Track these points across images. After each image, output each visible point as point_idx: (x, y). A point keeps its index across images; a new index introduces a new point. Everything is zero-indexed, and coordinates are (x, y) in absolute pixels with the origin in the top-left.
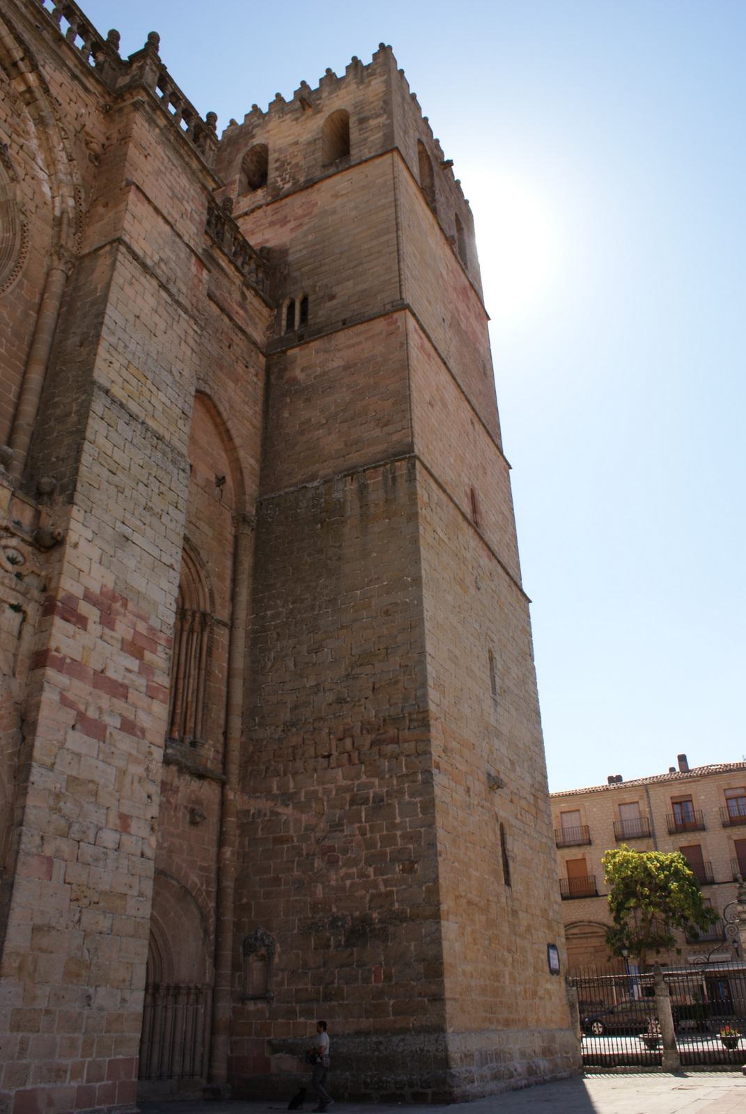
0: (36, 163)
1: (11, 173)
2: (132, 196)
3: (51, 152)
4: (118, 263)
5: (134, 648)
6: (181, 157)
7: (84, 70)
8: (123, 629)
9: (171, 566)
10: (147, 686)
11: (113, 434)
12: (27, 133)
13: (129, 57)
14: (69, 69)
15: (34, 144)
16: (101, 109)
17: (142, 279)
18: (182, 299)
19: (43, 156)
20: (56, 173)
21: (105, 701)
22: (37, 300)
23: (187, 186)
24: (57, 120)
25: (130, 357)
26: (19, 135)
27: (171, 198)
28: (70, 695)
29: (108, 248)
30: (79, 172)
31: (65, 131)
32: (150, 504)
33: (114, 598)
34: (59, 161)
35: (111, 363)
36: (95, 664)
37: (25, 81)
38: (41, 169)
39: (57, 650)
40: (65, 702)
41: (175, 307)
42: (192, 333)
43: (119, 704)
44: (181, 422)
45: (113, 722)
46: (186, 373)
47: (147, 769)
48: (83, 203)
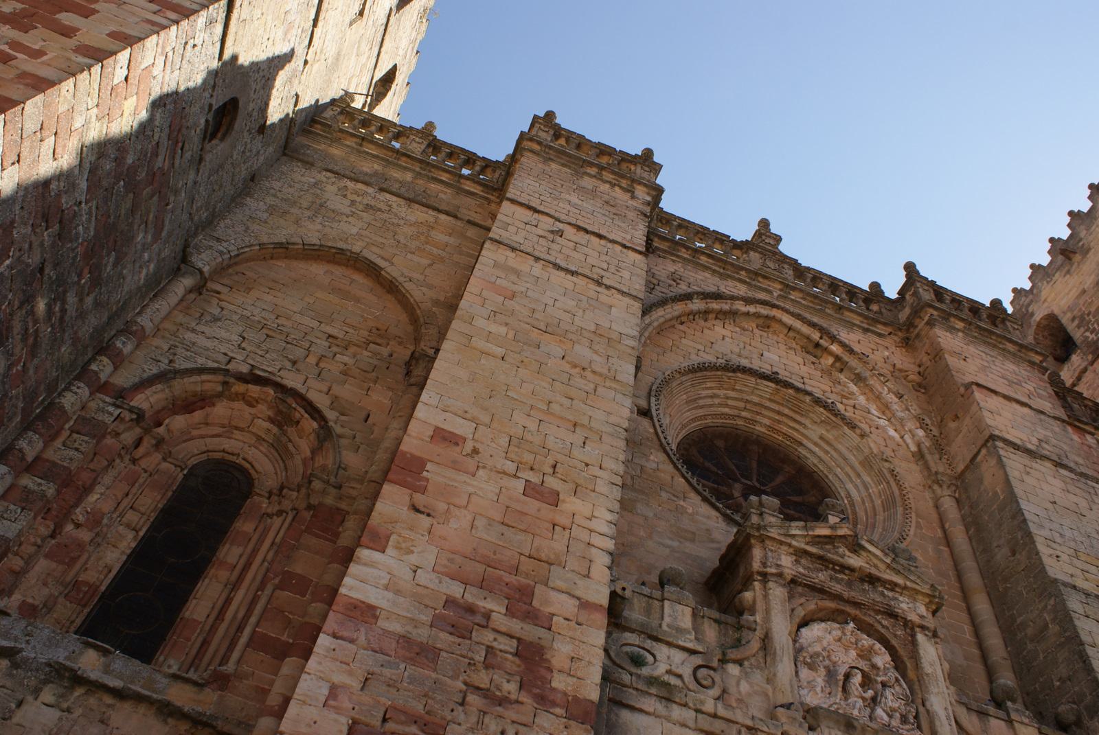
0: (873, 415)
1: (858, 431)
2: (978, 395)
3: (880, 399)
4: (1004, 459)
6: (994, 346)
7: (870, 321)
12: (853, 393)
13: (898, 293)
14: (859, 327)
15: (862, 400)
16: (901, 345)
17: (1034, 465)
18: (1083, 470)
19: (875, 407)
20: (894, 414)
22: (939, 533)
24: (871, 370)
26: (847, 398)
29: (984, 451)
30: (913, 403)
31: (882, 375)
34: (891, 403)
35: (1057, 557)
37: (831, 353)
38: (879, 418)
48: (932, 428)
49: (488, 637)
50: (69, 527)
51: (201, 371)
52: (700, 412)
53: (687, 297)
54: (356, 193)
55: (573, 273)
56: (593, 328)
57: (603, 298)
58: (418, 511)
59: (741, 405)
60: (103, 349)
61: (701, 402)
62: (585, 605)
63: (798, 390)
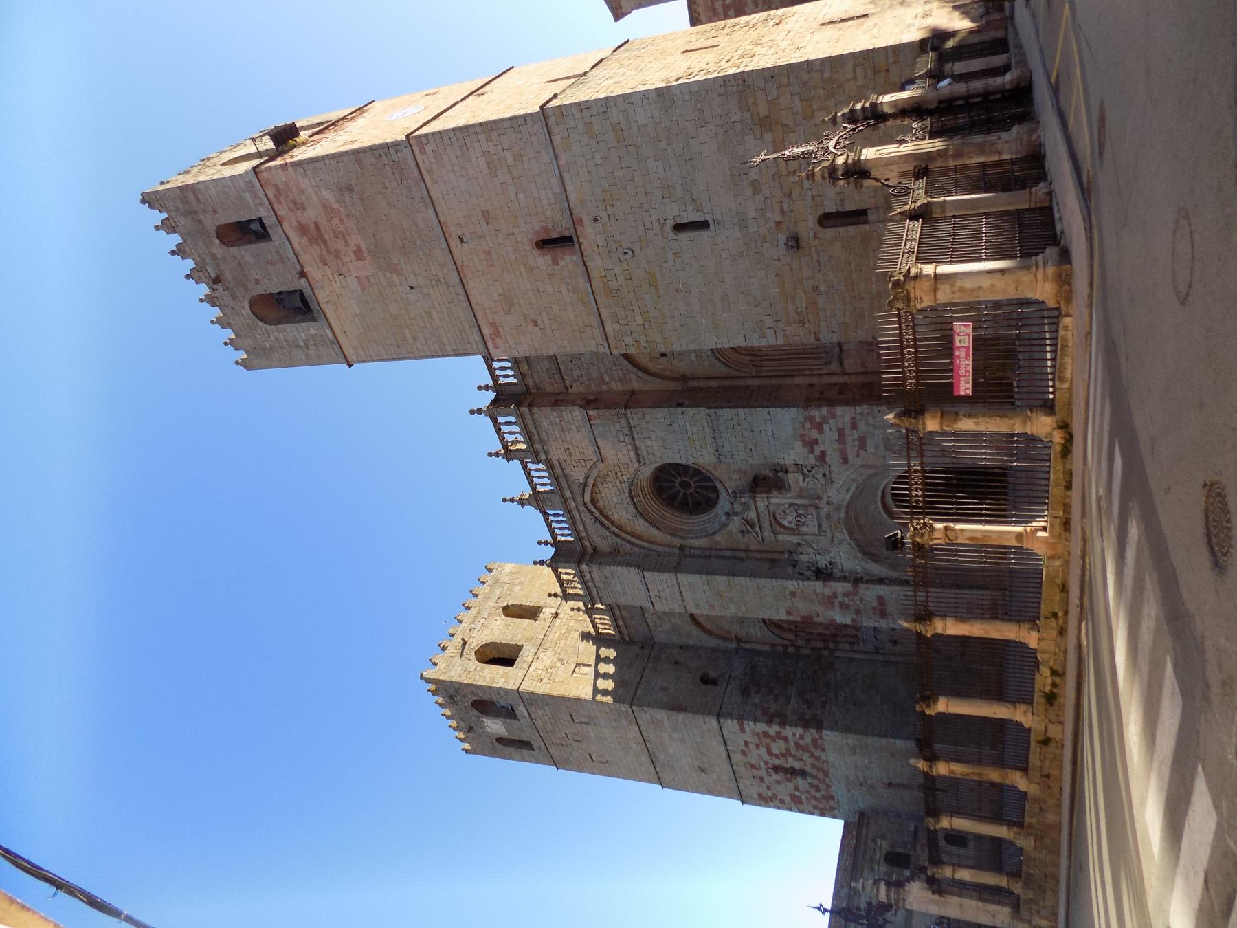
5: (819, 427)
8: (814, 434)
10: (832, 418)
17: (643, 448)
18: (624, 424)
21: (849, 439)
25: (689, 448)
33: (804, 441)
36: (836, 445)
40: (858, 456)
41: (633, 429)
43: (847, 432)
44: (691, 414)
45: (856, 434)
46: (660, 416)
47: (868, 414)
50: (833, 632)
51: (771, 631)
53: (614, 533)
54: (655, 623)
55: (681, 592)
60: (786, 653)
62: (824, 585)
63: (630, 490)
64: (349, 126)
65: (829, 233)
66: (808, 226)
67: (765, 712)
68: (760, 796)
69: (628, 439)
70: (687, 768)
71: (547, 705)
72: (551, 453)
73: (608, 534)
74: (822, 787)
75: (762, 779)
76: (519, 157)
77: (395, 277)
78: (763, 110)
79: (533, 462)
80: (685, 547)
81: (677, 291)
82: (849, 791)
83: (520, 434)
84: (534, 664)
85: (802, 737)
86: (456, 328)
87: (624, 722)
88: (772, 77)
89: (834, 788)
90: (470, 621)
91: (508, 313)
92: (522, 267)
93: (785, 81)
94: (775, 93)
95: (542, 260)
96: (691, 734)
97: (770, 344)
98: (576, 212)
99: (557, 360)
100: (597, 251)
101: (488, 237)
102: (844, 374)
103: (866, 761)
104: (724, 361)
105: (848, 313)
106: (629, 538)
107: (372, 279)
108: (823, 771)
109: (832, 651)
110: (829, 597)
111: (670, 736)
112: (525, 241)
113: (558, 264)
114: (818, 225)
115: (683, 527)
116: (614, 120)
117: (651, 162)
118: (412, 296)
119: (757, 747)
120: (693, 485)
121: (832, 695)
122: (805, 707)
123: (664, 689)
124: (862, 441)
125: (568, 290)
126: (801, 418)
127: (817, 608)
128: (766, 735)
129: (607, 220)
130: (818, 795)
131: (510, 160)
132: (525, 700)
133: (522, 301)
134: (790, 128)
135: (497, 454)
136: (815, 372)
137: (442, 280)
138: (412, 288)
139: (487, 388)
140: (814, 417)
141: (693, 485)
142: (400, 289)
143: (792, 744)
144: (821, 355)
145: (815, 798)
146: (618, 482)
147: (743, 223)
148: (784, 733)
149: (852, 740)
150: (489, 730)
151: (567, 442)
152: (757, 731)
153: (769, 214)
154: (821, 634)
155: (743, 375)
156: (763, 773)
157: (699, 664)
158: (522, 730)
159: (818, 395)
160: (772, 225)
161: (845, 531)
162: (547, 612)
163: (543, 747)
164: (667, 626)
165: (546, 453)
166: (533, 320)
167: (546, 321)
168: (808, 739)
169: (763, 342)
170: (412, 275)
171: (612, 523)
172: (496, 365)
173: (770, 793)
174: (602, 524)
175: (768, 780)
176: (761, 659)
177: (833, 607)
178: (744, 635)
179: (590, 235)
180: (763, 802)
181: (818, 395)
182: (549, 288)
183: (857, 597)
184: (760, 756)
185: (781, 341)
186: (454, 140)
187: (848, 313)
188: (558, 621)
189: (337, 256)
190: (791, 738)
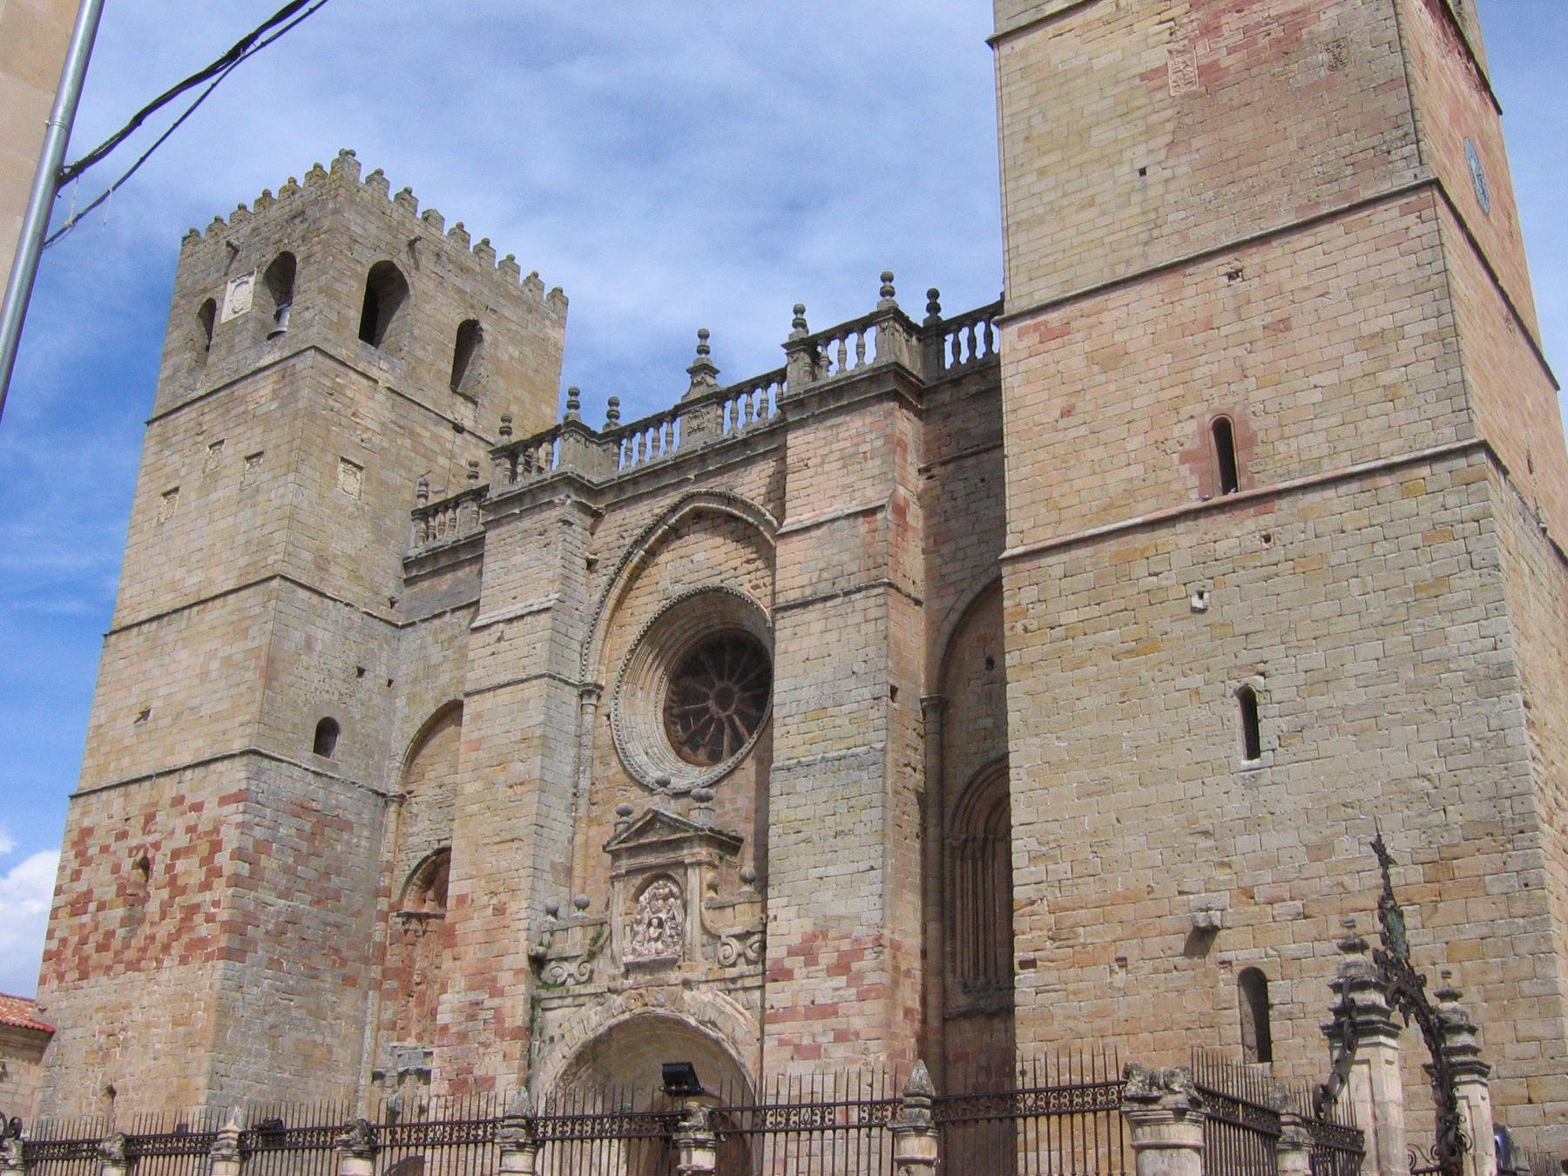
5: (841, 967)
8: (826, 958)
9: (872, 868)
11: (794, 800)
18: (855, 582)
21: (817, 1026)
23: (861, 423)
25: (804, 708)
27: (845, 466)
28: (786, 1037)
32: (839, 829)
36: (804, 1001)
39: (772, 1007)
40: (782, 1043)
41: (847, 599)
42: (872, 601)
43: (833, 1022)
44: (873, 714)
45: (826, 1039)
46: (871, 651)
49: (483, 1015)
52: (670, 653)
54: (442, 630)
56: (519, 737)
57: (527, 694)
58: (455, 959)
59: (696, 621)
61: (668, 645)
62: (517, 972)
64: (1454, 64)
65: (1229, 988)
66: (1237, 949)
67: (262, 847)
68: (88, 832)
69: (824, 589)
70: (147, 686)
71: (281, 406)
72: (800, 432)
73: (629, 541)
74: (107, 957)
75: (123, 835)
76: (1391, 394)
77: (1168, 138)
78: (1469, 865)
79: (780, 397)
80: (599, 697)
81: (1123, 694)
82: (98, 1010)
83: (842, 370)
84: (364, 381)
85: (210, 918)
86: (1059, 256)
87: (242, 562)
88: (1526, 885)
89: (103, 980)
90: (453, 253)
91: (1090, 359)
92: (1179, 390)
93: (1518, 908)
94: (1496, 889)
95: (1192, 431)
96: (218, 696)
97: (1015, 872)
98: (1283, 504)
99: (987, 450)
100: (1207, 538)
101: (1237, 327)
102: (945, 1020)
103: (158, 1046)
104: (975, 785)
105: (1071, 1023)
106: (621, 583)
107: (1160, 95)
108: (139, 961)
109: (378, 985)
110: (494, 980)
111: (213, 654)
112: (1230, 399)
113: (1183, 461)
114: (1242, 968)
115: (639, 694)
116: (1455, 582)
117: (1374, 648)
118: (1126, 173)
119: (191, 829)
120: (723, 715)
121: (291, 982)
122: (270, 927)
123: (309, 644)
124: (813, 1052)
125: (1131, 480)
126: (859, 931)
127: (472, 954)
128: (216, 847)
129: (1265, 561)
130: (90, 948)
131: (1386, 378)
132: (292, 362)
133: (1112, 387)
134: (1430, 917)
135: (800, 324)
136: (948, 965)
137: (1156, 233)
138: (1143, 172)
139: (934, 308)
140: (861, 959)
141: (723, 715)
142: (1141, 149)
143: (197, 898)
144: (982, 976)
145: (83, 941)
146: (737, 562)
147: (1252, 824)
148: (219, 884)
149: (203, 1019)
150: (231, 287)
151: (823, 463)
152: (223, 829)
153: (1267, 876)
154: (413, 962)
155: (947, 821)
156: (133, 842)
157: (358, 717)
158: (230, 351)
159: (903, 968)
160: (1247, 881)
161: (627, 1016)
162: (464, 413)
163: (196, 395)
164: (435, 654)
165: (801, 424)
166: (1073, 407)
167: (1072, 434)
168: (204, 930)
169: (1017, 860)
170: (1167, 174)
171: (652, 553)
172: (980, 329)
173: (93, 851)
174: (650, 530)
175: (121, 848)
176: (364, 843)
177: (471, 988)
178: (415, 809)
179: (1239, 531)
180: (75, 835)
181: (903, 968)
182: (1134, 443)
183: (492, 1036)
184: (172, 833)
185: (1019, 893)
186: (1428, 271)
187: (1071, 1023)
188: (449, 434)
189: (1210, 30)
190: (208, 896)
